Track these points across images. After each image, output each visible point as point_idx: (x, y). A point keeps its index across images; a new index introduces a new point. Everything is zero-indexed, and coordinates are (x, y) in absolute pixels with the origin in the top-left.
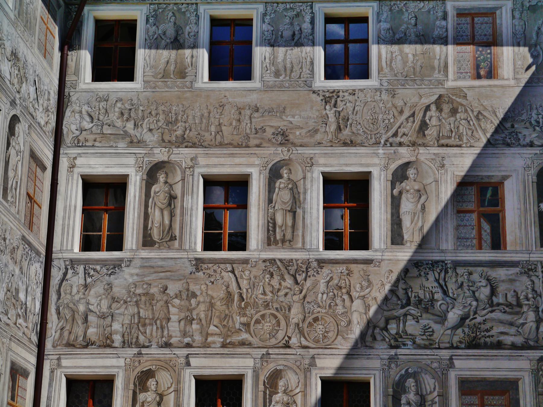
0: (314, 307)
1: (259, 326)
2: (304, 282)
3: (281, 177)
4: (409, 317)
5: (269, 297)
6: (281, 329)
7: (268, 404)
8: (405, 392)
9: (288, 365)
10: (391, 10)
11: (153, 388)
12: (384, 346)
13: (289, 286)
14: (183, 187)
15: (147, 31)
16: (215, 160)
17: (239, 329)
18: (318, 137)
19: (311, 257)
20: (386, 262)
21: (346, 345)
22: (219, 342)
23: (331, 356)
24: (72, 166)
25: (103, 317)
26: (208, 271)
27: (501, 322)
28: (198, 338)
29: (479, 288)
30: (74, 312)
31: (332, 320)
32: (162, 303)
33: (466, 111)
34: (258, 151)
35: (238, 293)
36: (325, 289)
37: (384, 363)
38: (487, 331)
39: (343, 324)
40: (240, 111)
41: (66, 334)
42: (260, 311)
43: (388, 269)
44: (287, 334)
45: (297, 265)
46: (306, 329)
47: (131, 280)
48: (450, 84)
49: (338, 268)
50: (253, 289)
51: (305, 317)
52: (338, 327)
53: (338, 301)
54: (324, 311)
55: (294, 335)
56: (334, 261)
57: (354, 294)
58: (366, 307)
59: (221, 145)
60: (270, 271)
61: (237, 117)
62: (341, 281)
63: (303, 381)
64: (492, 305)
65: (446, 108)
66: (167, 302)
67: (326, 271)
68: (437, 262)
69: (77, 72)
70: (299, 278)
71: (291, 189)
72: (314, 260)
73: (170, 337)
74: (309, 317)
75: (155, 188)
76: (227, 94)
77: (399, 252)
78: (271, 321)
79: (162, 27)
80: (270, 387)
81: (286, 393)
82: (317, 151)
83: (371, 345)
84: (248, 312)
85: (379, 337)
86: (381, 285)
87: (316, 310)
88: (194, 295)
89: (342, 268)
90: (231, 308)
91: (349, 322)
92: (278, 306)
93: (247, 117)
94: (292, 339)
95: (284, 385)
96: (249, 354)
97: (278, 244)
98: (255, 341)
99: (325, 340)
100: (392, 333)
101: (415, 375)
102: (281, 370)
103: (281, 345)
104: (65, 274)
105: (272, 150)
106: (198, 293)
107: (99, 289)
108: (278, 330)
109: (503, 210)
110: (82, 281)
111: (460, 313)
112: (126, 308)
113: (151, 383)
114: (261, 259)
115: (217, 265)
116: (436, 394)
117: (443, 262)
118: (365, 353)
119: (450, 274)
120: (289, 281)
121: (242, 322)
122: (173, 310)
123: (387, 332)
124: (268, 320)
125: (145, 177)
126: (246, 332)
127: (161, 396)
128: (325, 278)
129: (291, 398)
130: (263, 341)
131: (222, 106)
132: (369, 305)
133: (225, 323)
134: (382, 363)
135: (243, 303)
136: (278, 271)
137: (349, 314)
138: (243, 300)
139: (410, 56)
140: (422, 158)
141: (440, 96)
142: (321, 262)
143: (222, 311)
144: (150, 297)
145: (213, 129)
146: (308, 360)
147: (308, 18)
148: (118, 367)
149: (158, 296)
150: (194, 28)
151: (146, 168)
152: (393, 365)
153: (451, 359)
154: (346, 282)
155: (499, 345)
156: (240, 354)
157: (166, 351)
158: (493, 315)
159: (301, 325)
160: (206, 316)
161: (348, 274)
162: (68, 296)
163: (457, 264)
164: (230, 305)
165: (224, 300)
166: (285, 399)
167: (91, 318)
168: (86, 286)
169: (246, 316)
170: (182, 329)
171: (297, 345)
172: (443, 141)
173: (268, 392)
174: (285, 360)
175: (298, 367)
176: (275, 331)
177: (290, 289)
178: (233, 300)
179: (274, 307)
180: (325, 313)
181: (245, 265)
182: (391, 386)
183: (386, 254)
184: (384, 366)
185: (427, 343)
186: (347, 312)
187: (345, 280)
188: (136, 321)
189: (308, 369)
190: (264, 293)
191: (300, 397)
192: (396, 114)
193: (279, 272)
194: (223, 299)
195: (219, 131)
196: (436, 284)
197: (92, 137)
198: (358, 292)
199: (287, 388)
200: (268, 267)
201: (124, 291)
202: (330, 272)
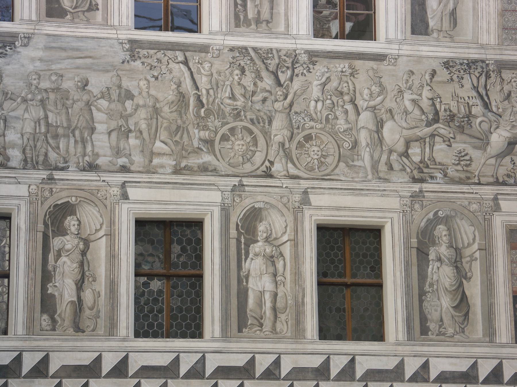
0: (305, 121)
1: (227, 145)
2: (290, 83)
4: (437, 139)
6: (258, 149)
7: (243, 257)
8: (434, 244)
9: (271, 202)
11: (73, 229)
12: (404, 178)
13: (268, 88)
17: (198, 148)
19: (299, 46)
20: (405, 58)
21: (351, 176)
22: (170, 165)
23: (331, 191)
26: (149, 61)
28: (138, 159)
31: (331, 139)
32: (80, 104)
35: (194, 94)
36: (320, 94)
37: (405, 202)
39: (346, 145)
42: (227, 123)
43: (408, 69)
45: (279, 57)
46: (294, 153)
47: (31, 68)
49: (337, 65)
50: (217, 90)
51: (292, 134)
52: (339, 150)
53: (339, 113)
54: (319, 126)
55: (277, 159)
56: (332, 55)
57: (361, 103)
58: (378, 122)
60: (240, 64)
62: (342, 83)
63: (292, 225)
66: (88, 104)
67: (320, 68)
68: (475, 62)
70: (282, 78)
72: (302, 52)
73: (97, 155)
74: (299, 133)
77: (422, 45)
78: (245, 138)
80: (246, 233)
81: (269, 242)
83: (386, 177)
84: (210, 124)
85: (396, 166)
86: (399, 92)
87: (308, 125)
88: (130, 96)
89: (343, 65)
90: (185, 117)
91: (355, 144)
92: (254, 117)
94: (275, 165)
95: (265, 230)
96: (213, 185)
97: (251, 25)
98: (222, 166)
99: (323, 168)
100: (414, 160)
101: (447, 220)
102: (260, 209)
103: (259, 172)
106: (135, 92)
108: (256, 152)
111: (507, 134)
112: (26, 110)
113: (71, 223)
114: (227, 47)
115: (162, 52)
116: (476, 246)
117: (483, 61)
118: (378, 188)
119: (492, 80)
120: (268, 81)
121: (202, 138)
122: (98, 116)
123: (408, 159)
124: (240, 136)
126: (208, 153)
127: (87, 242)
128: (320, 78)
129: (276, 250)
130: (234, 167)
132: (382, 120)
133: (177, 138)
134: (401, 202)
135: (203, 110)
136: (252, 65)
137: (354, 132)
138: (203, 106)
143: (173, 120)
144: (65, 95)
146: (299, 196)
148: (18, 197)
149: (75, 95)
152: (417, 206)
153: (496, 199)
154: (349, 86)
156: (201, 184)
157: (91, 176)
159: (287, 146)
160: (149, 126)
161: (352, 75)
164: (183, 111)
165: (174, 104)
166: (268, 250)
169: (207, 130)
170: (114, 143)
171: (282, 174)
173: (243, 240)
174: (266, 194)
175: (285, 205)
176: (250, 153)
177: (270, 92)
178: (187, 105)
179: (248, 117)
180: (321, 129)
181: (203, 55)
182: (414, 235)
183: (405, 47)
184: (405, 207)
185: (463, 176)
186: (351, 129)
187: (348, 83)
188: (43, 130)
189: (299, 208)
190: (233, 97)
191: (289, 248)
193: (253, 66)
194: (172, 102)
196: (475, 94)
198: (366, 101)
199: (270, 235)
200: (238, 59)
201: (21, 84)
202: (326, 70)
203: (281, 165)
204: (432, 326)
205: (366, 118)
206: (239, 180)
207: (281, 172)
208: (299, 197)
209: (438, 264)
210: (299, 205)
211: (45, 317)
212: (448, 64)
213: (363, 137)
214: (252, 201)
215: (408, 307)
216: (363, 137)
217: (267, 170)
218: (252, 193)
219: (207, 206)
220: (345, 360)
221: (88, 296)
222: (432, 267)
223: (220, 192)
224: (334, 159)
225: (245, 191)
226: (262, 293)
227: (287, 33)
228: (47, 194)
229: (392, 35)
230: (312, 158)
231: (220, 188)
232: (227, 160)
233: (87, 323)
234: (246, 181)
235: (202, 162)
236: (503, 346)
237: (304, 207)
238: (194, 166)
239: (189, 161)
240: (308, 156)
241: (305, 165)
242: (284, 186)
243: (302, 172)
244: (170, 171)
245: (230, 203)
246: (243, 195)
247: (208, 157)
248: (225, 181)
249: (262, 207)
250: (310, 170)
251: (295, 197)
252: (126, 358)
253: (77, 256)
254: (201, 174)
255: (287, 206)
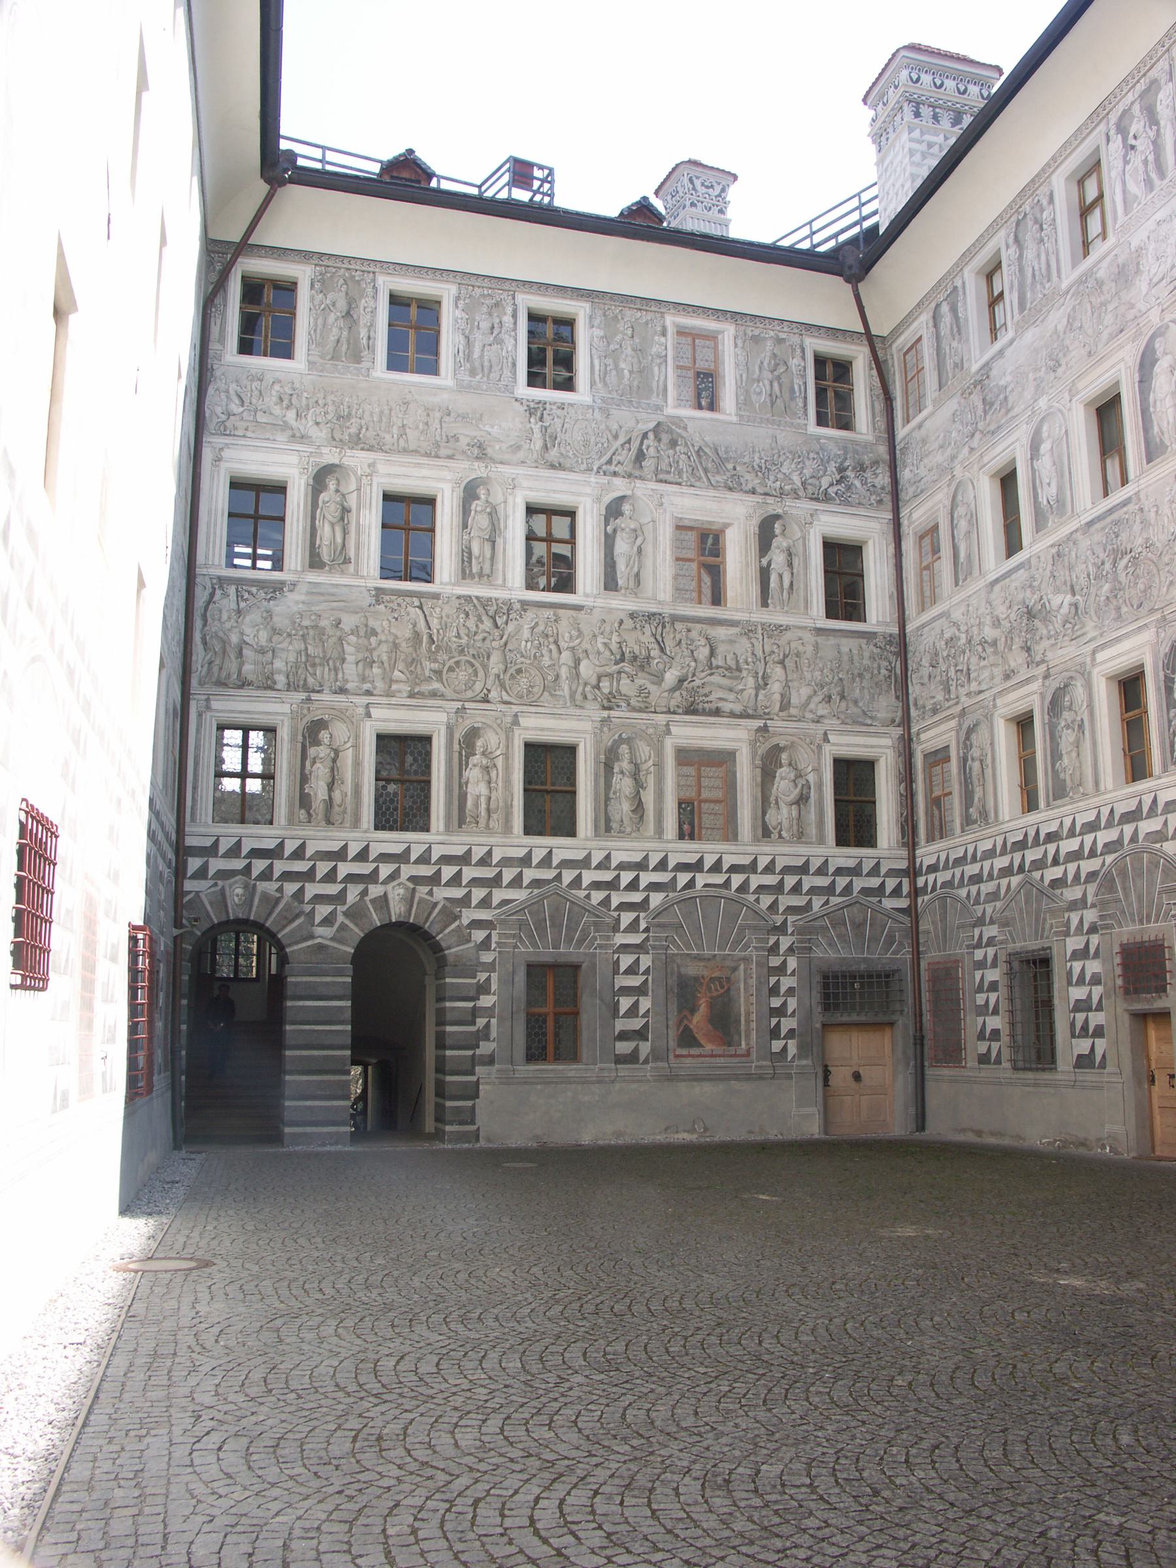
1: (453, 675)
3: (478, 498)
5: (465, 640)
8: (618, 760)
10: (604, 315)
11: (326, 741)
14: (359, 497)
15: (312, 299)
16: (396, 470)
18: (521, 455)
24: (218, 459)
25: (262, 651)
26: (391, 605)
27: (720, 687)
28: (380, 684)
29: (697, 647)
30: (224, 642)
32: (334, 639)
33: (686, 444)
34: (450, 463)
38: (706, 695)
39: (549, 678)
40: (428, 411)
41: (215, 669)
46: (507, 682)
47: (295, 609)
48: (671, 410)
54: (528, 662)
57: (562, 644)
59: (405, 451)
61: (424, 419)
64: (711, 668)
65: (665, 438)
66: (340, 639)
67: (530, 615)
68: (654, 614)
69: (222, 339)
70: (499, 621)
71: (490, 514)
73: (347, 681)
75: (323, 497)
76: (412, 389)
79: (330, 296)
82: (520, 470)
85: (590, 696)
88: (375, 633)
89: (549, 613)
91: (557, 677)
93: (437, 421)
98: (448, 692)
101: (629, 741)
103: (478, 698)
104: (212, 595)
105: (466, 464)
106: (379, 630)
107: (254, 616)
109: (724, 562)
110: (233, 606)
112: (290, 643)
113: (324, 735)
116: (651, 762)
119: (667, 629)
120: (487, 624)
122: (348, 649)
125: (311, 481)
131: (407, 403)
133: (412, 669)
139: (626, 372)
140: (639, 493)
141: (659, 424)
142: (525, 605)
144: (322, 632)
145: (395, 430)
147: (509, 310)
150: (372, 303)
151: (312, 471)
152: (605, 729)
153: (667, 725)
155: (717, 712)
157: (341, 697)
158: (713, 679)
160: (390, 658)
161: (556, 621)
162: (216, 623)
163: (675, 619)
166: (484, 762)
167: (247, 652)
168: (239, 612)
170: (360, 671)
172: (661, 476)
174: (484, 716)
178: (421, 642)
182: (603, 752)
185: (642, 705)
188: (303, 659)
190: (458, 636)
192: (610, 438)
195: (403, 434)
197: (243, 424)
201: (287, 622)
204: (614, 825)
205: (566, 656)
209: (620, 776)
211: (303, 811)
212: (632, 615)
213: (564, 672)
215: (596, 810)
216: (564, 672)
220: (544, 852)
221: (337, 795)
222: (616, 779)
226: (478, 797)
227: (504, 585)
228: (305, 711)
229: (588, 590)
233: (336, 818)
234: (467, 705)
236: (668, 842)
244: (405, 695)
252: (368, 846)
253: (329, 763)
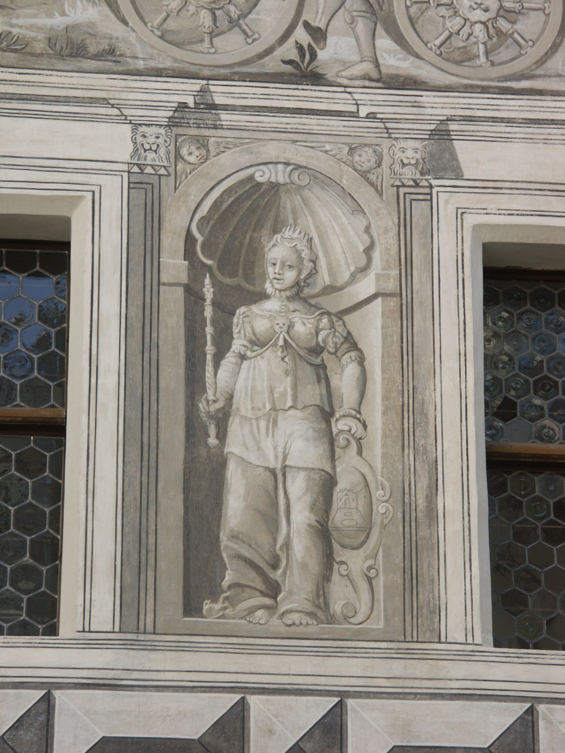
7: (210, 349)
9: (313, 164)
23: (534, 130)
44: (306, 16)
55: (339, 22)
63: (393, 242)
80: (221, 267)
81: (305, 300)
94: (331, 40)
95: (292, 259)
96: (105, 102)
99: (503, 54)
102: (274, 187)
129: (332, 326)
130: (179, 45)
146: (418, 144)
156: (57, 100)
171: (358, 70)
173: (208, 292)
175: (364, 175)
189: (417, 185)
191: (379, 322)
199: (310, 275)
203: (352, 41)
206: (198, 88)
207: (353, 64)
208: (416, 150)
210: (418, 176)
214: (246, 160)
217: (302, 56)
218: (245, 134)
219: (77, 171)
223: (129, 127)
224: (546, 23)
225: (221, 127)
230: (466, 20)
231: (125, 112)
232: (156, 23)
235: (62, 26)
237: (434, 182)
238: (34, 39)
239: (14, 21)
240: (451, 12)
241: (438, 42)
242: (363, 111)
243: (428, 67)
245: (165, 164)
246: (212, 140)
247: (85, 9)
248: (146, 91)
249: (281, 180)
250: (459, 58)
251: (403, 150)
254: (60, 65)
255: (372, 177)
